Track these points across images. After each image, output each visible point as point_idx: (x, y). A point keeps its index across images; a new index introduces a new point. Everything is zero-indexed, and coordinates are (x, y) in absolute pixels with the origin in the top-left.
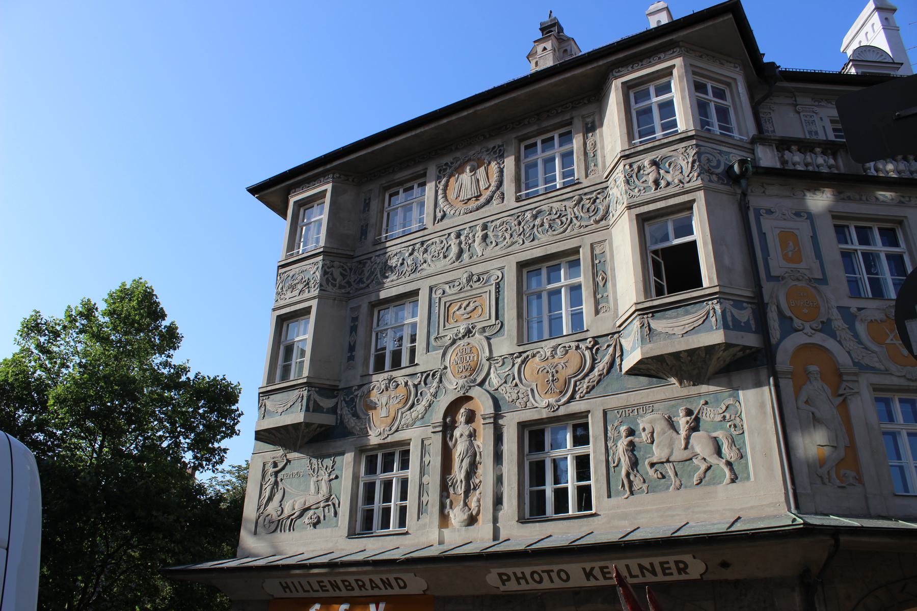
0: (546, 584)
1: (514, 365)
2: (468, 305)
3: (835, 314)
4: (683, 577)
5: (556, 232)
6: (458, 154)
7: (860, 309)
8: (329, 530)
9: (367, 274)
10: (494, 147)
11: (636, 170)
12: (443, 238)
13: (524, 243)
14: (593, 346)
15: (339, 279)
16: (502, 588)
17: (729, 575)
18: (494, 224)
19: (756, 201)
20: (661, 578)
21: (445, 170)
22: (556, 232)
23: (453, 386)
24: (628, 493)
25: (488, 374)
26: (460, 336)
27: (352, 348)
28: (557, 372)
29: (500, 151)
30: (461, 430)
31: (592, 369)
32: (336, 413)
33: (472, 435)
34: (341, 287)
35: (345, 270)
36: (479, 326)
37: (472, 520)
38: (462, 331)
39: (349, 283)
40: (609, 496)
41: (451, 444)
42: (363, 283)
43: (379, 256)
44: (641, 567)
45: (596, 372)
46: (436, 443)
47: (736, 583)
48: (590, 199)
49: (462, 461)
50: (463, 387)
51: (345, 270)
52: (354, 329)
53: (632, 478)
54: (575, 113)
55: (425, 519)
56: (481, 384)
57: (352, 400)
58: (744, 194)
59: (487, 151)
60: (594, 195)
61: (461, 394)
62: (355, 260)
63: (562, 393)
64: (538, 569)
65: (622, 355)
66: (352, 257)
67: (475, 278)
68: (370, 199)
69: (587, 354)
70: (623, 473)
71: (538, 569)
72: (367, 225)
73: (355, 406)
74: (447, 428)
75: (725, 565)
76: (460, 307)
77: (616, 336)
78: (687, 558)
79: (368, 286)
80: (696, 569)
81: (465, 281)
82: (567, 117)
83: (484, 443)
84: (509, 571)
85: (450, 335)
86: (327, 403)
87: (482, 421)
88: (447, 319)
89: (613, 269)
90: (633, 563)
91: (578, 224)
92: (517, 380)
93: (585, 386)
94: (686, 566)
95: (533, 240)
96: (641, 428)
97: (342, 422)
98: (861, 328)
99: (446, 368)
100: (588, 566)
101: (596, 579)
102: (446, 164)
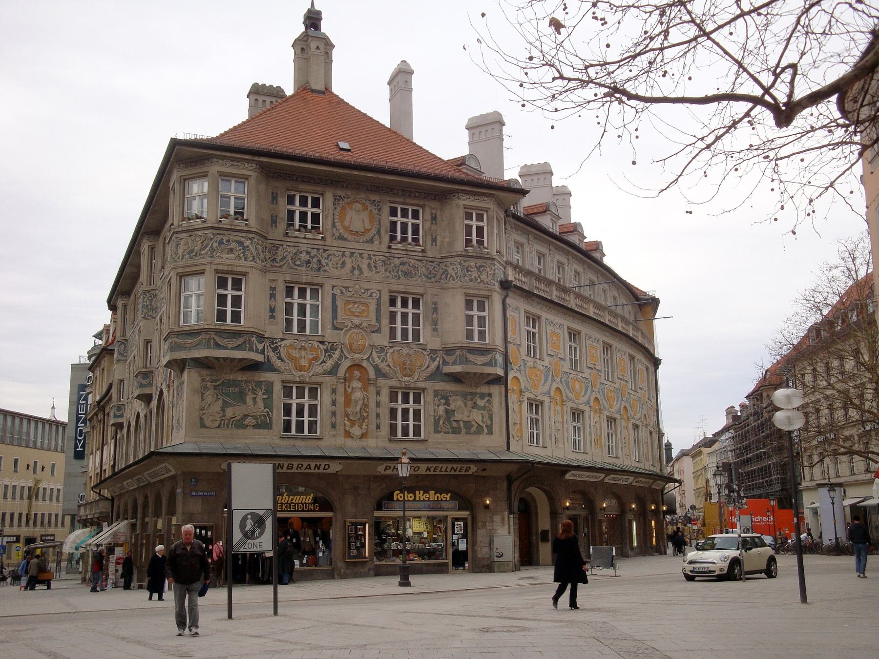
6: (349, 193)
8: (266, 431)
9: (280, 257)
19: (508, 301)
20: (457, 473)
21: (339, 200)
27: (272, 310)
31: (428, 367)
34: (263, 261)
41: (349, 390)
44: (452, 468)
45: (430, 369)
47: (484, 477)
52: (272, 296)
54: (426, 203)
56: (368, 359)
57: (276, 348)
58: (506, 296)
62: (269, 241)
66: (266, 238)
72: (276, 216)
75: (484, 470)
79: (281, 267)
80: (473, 468)
82: (421, 203)
84: (392, 465)
90: (450, 466)
97: (269, 361)
98: (527, 370)
100: (430, 466)
102: (340, 196)
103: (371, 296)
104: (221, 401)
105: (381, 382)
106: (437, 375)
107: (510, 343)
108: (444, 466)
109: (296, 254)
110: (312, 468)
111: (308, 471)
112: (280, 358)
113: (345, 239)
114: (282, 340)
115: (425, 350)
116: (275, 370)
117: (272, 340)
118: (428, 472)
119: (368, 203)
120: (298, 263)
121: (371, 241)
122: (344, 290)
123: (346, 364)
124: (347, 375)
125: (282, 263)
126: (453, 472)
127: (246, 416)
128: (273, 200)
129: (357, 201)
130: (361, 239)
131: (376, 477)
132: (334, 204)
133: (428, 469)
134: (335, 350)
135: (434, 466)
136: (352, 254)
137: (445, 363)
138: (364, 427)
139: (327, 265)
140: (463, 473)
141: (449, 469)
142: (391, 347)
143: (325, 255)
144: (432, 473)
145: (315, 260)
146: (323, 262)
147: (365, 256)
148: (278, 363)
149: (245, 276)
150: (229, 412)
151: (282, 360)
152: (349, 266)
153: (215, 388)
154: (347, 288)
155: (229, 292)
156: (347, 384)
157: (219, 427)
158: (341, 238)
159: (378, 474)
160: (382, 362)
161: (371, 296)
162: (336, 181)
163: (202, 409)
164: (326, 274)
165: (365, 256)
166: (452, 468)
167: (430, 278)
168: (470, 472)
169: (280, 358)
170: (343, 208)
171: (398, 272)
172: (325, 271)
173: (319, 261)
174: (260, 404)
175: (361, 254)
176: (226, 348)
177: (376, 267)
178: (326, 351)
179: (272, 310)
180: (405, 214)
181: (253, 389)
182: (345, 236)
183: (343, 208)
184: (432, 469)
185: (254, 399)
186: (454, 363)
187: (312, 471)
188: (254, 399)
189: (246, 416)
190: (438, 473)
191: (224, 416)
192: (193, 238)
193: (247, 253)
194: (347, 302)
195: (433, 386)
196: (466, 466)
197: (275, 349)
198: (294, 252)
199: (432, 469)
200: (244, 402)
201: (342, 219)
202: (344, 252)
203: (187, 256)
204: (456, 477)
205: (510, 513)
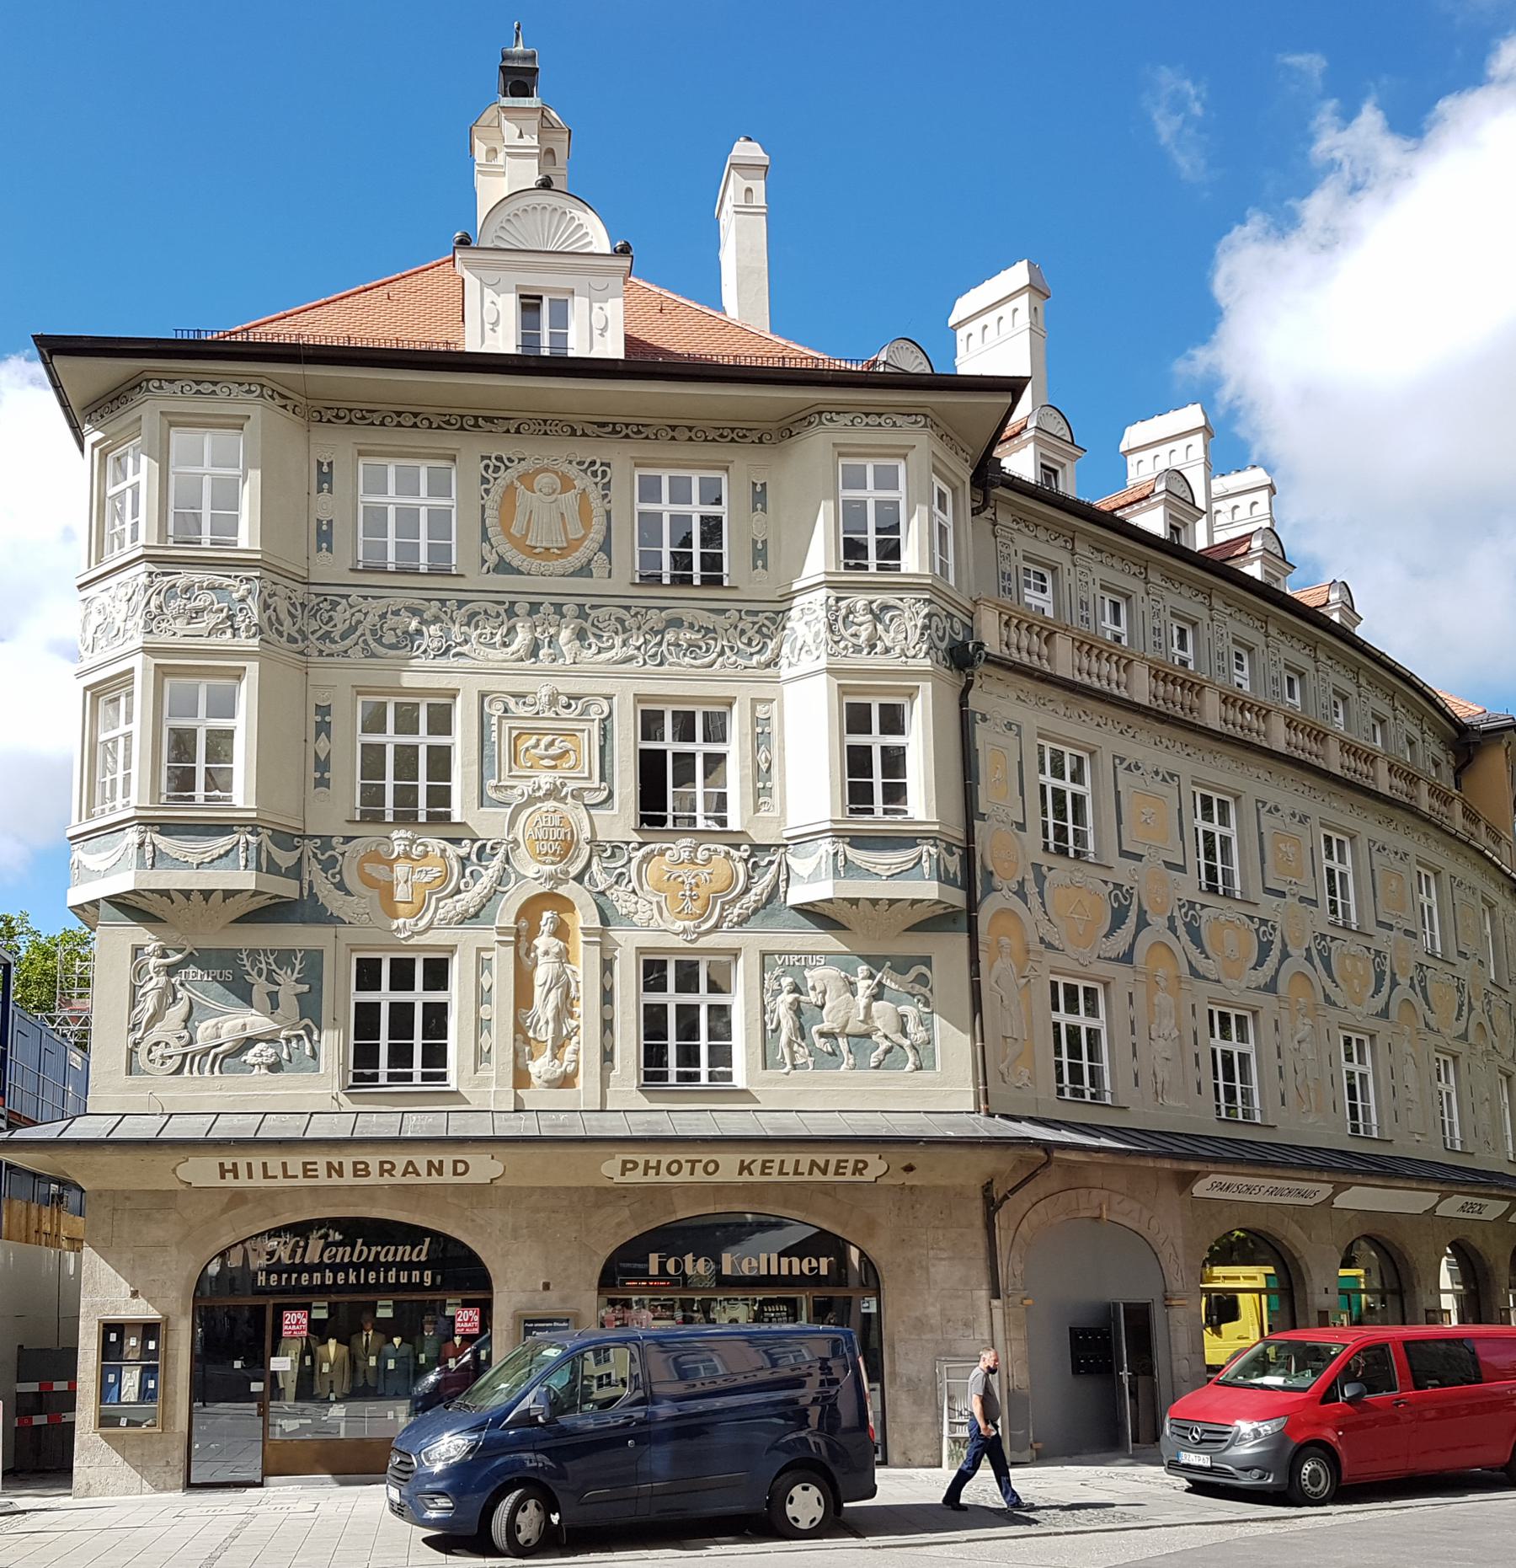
0: (684, 1177)
1: (630, 859)
2: (552, 744)
3: (1030, 876)
4: (858, 1178)
5: (698, 662)
7: (1050, 869)
9: (341, 627)
10: (593, 463)
11: (843, 612)
12: (501, 609)
13: (645, 663)
14: (750, 856)
15: (287, 621)
16: (618, 1179)
17: (911, 1179)
18: (593, 613)
20: (830, 1177)
21: (497, 469)
22: (698, 662)
23: (532, 873)
24: (789, 1066)
25: (588, 864)
26: (541, 793)
27: (323, 765)
28: (697, 885)
29: (604, 473)
30: (543, 942)
31: (747, 890)
32: (299, 878)
33: (564, 956)
35: (293, 605)
36: (572, 785)
37: (566, 1081)
38: (545, 787)
39: (300, 631)
40: (765, 1068)
42: (333, 641)
43: (365, 598)
44: (813, 1163)
45: (751, 897)
46: (503, 961)
48: (754, 623)
49: (549, 990)
50: (551, 877)
51: (293, 605)
53: (796, 1047)
55: (490, 1071)
56: (579, 878)
59: (580, 463)
60: (761, 618)
61: (546, 888)
63: (702, 917)
64: (682, 1158)
65: (788, 880)
67: (563, 700)
68: (330, 464)
69: (741, 867)
70: (784, 1039)
71: (682, 1158)
73: (340, 872)
74: (522, 939)
76: (536, 746)
77: (782, 850)
78: (871, 1158)
81: (545, 699)
83: (584, 969)
84: (640, 1159)
85: (525, 787)
86: (285, 859)
87: (582, 938)
88: (514, 758)
89: (782, 749)
90: (805, 1159)
91: (733, 658)
92: (635, 883)
93: (736, 911)
94: (866, 1166)
95: (661, 664)
96: (810, 984)
99: (515, 841)
100: (748, 1158)
101: (751, 1174)
102: (499, 459)
107: (982, 817)
108: (790, 1159)
109: (383, 616)
110: (398, 1171)
111: (411, 1179)
112: (340, 886)
114: (348, 839)
115: (737, 847)
117: (326, 841)
118: (746, 1177)
119: (573, 471)
121: (584, 571)
122: (511, 702)
124: (524, 924)
126: (817, 1176)
128: (320, 483)
129: (546, 470)
130: (557, 565)
131: (600, 1191)
132: (485, 480)
133: (744, 1168)
135: (761, 1158)
136: (534, 608)
140: (848, 1177)
141: (804, 1168)
142: (642, 845)
143: (461, 615)
144: (757, 1178)
147: (570, 609)
150: (204, 1032)
156: (523, 945)
157: (179, 1071)
158: (503, 567)
159: (609, 1184)
162: (487, 419)
164: (462, 661)
165: (570, 609)
166: (813, 1163)
168: (869, 1176)
169: (340, 886)
170: (510, 489)
171: (660, 644)
175: (558, 608)
178: (464, 861)
180: (680, 493)
182: (515, 563)
183: (510, 489)
184: (756, 1168)
185: (273, 997)
186: (814, 877)
187: (424, 1179)
188: (273, 997)
190: (775, 1177)
191: (191, 1042)
192: (111, 592)
196: (852, 1158)
197: (329, 865)
199: (756, 1168)
201: (506, 519)
202: (513, 603)
203: (103, 643)
204: (826, 1189)
205: (995, 1294)
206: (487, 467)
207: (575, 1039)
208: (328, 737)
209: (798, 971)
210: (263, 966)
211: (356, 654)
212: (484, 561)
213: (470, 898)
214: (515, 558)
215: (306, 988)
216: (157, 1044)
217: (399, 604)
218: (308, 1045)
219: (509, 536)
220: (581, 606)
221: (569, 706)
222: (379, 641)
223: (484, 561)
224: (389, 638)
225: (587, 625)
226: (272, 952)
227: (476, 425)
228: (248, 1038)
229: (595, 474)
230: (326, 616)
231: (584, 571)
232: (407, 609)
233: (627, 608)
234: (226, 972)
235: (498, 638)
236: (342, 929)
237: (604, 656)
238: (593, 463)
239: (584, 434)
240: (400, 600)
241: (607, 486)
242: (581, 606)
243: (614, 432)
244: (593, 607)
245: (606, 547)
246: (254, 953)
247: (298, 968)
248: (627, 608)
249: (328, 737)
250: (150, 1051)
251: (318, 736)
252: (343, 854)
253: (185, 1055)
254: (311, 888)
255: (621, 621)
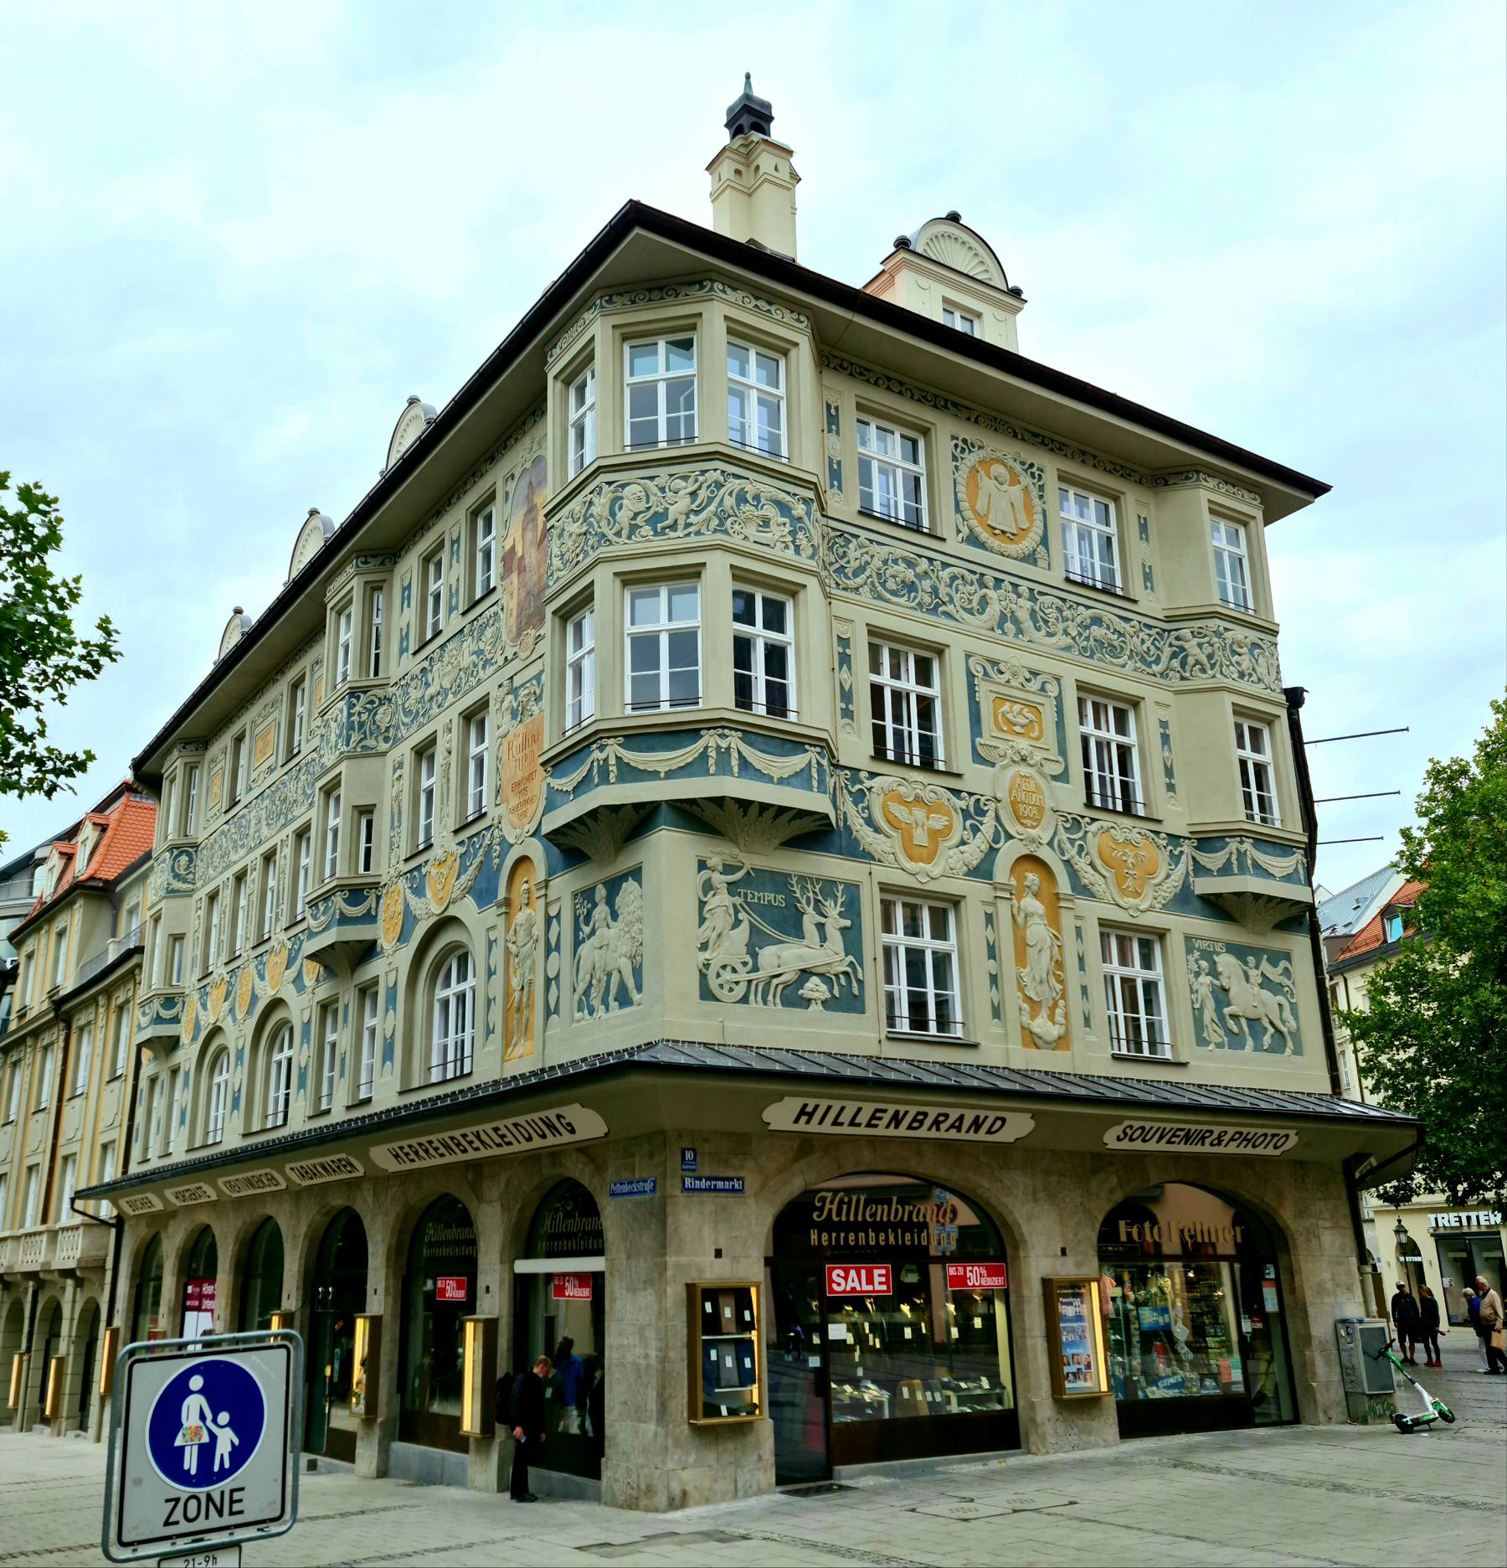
9: (855, 565)
10: (1032, 465)
18: (1041, 599)
27: (847, 696)
43: (871, 541)
73: (868, 808)
102: (965, 441)
103: (1043, 689)
104: (745, 926)
105: (1082, 904)
106: (1184, 900)
109: (885, 562)
112: (869, 821)
113: (982, 546)
114: (873, 775)
116: (855, 851)
120: (891, 585)
122: (988, 667)
123: (1009, 852)
125: (860, 580)
127: (805, 974)
130: (1012, 548)
134: (983, 813)
136: (998, 582)
137: (1199, 869)
138: (1059, 1018)
139: (951, 601)
145: (926, 584)
146: (943, 590)
148: (867, 837)
149: (794, 595)
151: (877, 830)
152: (994, 610)
153: (732, 888)
154: (994, 663)
155: (760, 634)
157: (744, 1000)
160: (1079, 854)
161: (1043, 689)
163: (704, 947)
167: (1149, 665)
169: (869, 821)
170: (974, 470)
172: (947, 614)
173: (935, 591)
174: (836, 940)
176: (768, 779)
177: (1046, 622)
179: (847, 696)
181: (817, 901)
185: (820, 927)
188: (820, 927)
189: (805, 974)
191: (755, 969)
193: (800, 535)
194: (1001, 698)
195: (1181, 925)
197: (859, 797)
198: (884, 556)
200: (799, 933)
206: (956, 446)
207: (1061, 1002)
208: (849, 668)
209: (1207, 955)
210: (811, 895)
211: (866, 595)
212: (959, 531)
213: (975, 851)
214: (984, 536)
215: (848, 923)
216: (724, 967)
217: (899, 553)
218: (855, 984)
219: (976, 512)
220: (1031, 590)
221: (1028, 680)
222: (883, 584)
223: (959, 531)
224: (891, 585)
225: (1037, 608)
226: (818, 880)
227: (946, 407)
228: (803, 971)
229: (1033, 475)
230: (841, 551)
231: (1030, 558)
232: (904, 559)
233: (1064, 600)
234: (779, 897)
235: (975, 604)
236: (875, 868)
237: (1053, 640)
238: (1032, 465)
239: (1023, 439)
240: (902, 550)
241: (1041, 488)
242: (1031, 590)
243: (1043, 444)
244: (1041, 593)
245: (1044, 541)
246: (802, 879)
247: (840, 900)
248: (1064, 600)
249: (849, 668)
250: (718, 975)
251: (841, 668)
252: (869, 789)
253: (750, 982)
254: (845, 820)
255: (1060, 610)
